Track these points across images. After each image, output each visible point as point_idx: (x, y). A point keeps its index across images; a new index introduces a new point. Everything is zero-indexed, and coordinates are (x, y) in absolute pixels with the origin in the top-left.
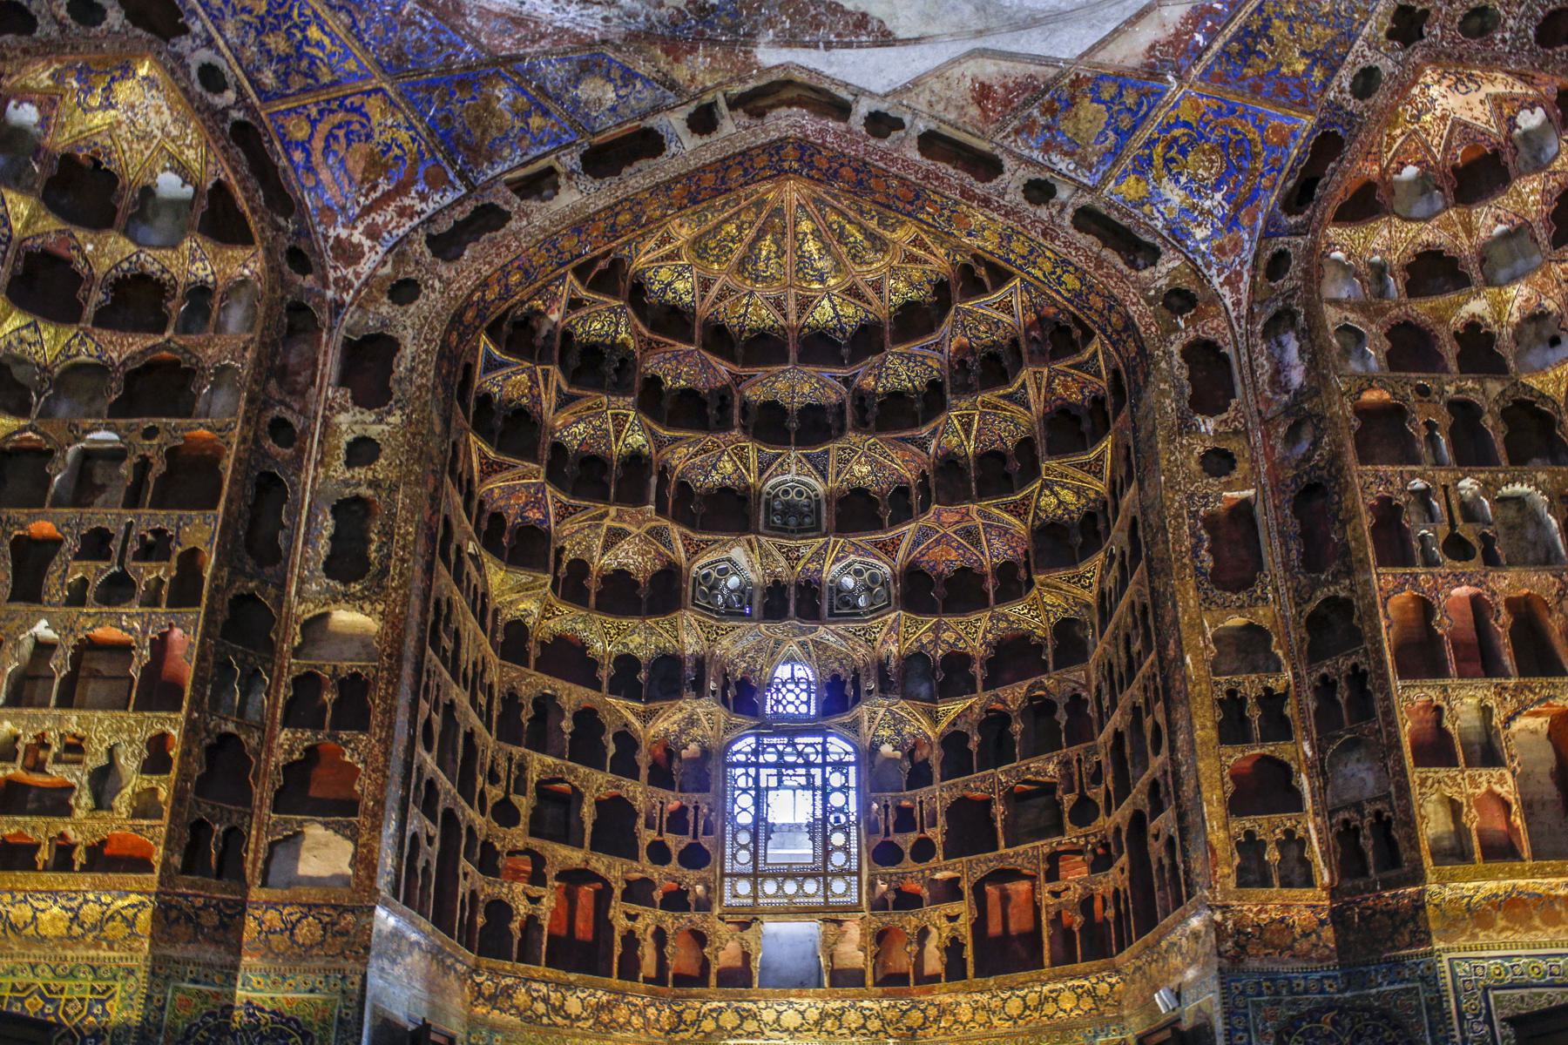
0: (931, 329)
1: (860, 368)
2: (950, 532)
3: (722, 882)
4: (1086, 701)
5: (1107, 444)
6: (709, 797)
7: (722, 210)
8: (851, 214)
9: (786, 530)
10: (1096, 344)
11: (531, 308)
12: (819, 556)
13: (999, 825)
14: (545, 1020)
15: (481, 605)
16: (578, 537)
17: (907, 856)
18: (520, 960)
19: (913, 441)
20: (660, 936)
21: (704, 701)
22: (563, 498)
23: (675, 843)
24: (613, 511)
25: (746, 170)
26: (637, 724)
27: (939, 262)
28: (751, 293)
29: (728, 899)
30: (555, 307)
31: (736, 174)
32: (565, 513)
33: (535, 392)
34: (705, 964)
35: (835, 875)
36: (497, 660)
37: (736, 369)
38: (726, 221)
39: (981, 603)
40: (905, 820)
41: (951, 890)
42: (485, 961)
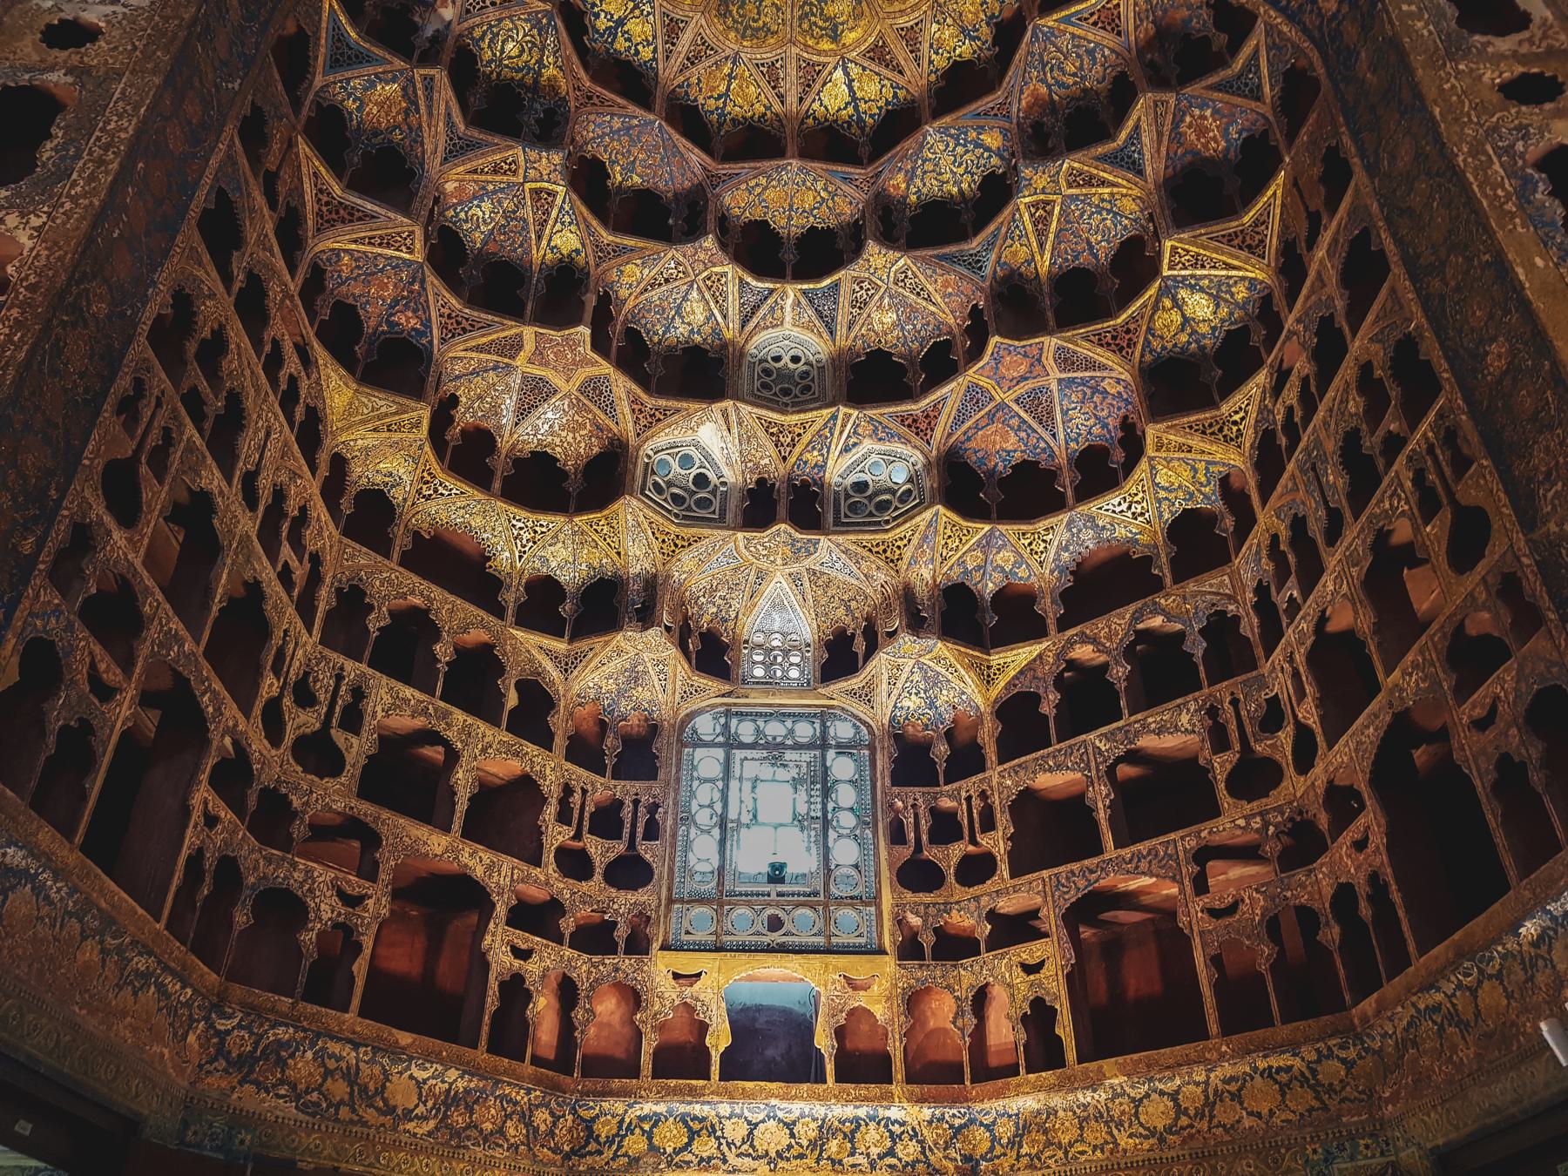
0: (990, 88)
2: (1009, 398)
3: (668, 909)
5: (1276, 188)
6: (657, 787)
12: (821, 441)
13: (1102, 816)
14: (344, 1112)
15: (310, 432)
17: (951, 879)
18: (310, 997)
20: (568, 992)
21: (654, 635)
23: (600, 850)
24: (529, 333)
26: (554, 673)
32: (456, 328)
33: (413, 120)
35: (841, 901)
36: (336, 533)
39: (1056, 504)
42: (238, 990)
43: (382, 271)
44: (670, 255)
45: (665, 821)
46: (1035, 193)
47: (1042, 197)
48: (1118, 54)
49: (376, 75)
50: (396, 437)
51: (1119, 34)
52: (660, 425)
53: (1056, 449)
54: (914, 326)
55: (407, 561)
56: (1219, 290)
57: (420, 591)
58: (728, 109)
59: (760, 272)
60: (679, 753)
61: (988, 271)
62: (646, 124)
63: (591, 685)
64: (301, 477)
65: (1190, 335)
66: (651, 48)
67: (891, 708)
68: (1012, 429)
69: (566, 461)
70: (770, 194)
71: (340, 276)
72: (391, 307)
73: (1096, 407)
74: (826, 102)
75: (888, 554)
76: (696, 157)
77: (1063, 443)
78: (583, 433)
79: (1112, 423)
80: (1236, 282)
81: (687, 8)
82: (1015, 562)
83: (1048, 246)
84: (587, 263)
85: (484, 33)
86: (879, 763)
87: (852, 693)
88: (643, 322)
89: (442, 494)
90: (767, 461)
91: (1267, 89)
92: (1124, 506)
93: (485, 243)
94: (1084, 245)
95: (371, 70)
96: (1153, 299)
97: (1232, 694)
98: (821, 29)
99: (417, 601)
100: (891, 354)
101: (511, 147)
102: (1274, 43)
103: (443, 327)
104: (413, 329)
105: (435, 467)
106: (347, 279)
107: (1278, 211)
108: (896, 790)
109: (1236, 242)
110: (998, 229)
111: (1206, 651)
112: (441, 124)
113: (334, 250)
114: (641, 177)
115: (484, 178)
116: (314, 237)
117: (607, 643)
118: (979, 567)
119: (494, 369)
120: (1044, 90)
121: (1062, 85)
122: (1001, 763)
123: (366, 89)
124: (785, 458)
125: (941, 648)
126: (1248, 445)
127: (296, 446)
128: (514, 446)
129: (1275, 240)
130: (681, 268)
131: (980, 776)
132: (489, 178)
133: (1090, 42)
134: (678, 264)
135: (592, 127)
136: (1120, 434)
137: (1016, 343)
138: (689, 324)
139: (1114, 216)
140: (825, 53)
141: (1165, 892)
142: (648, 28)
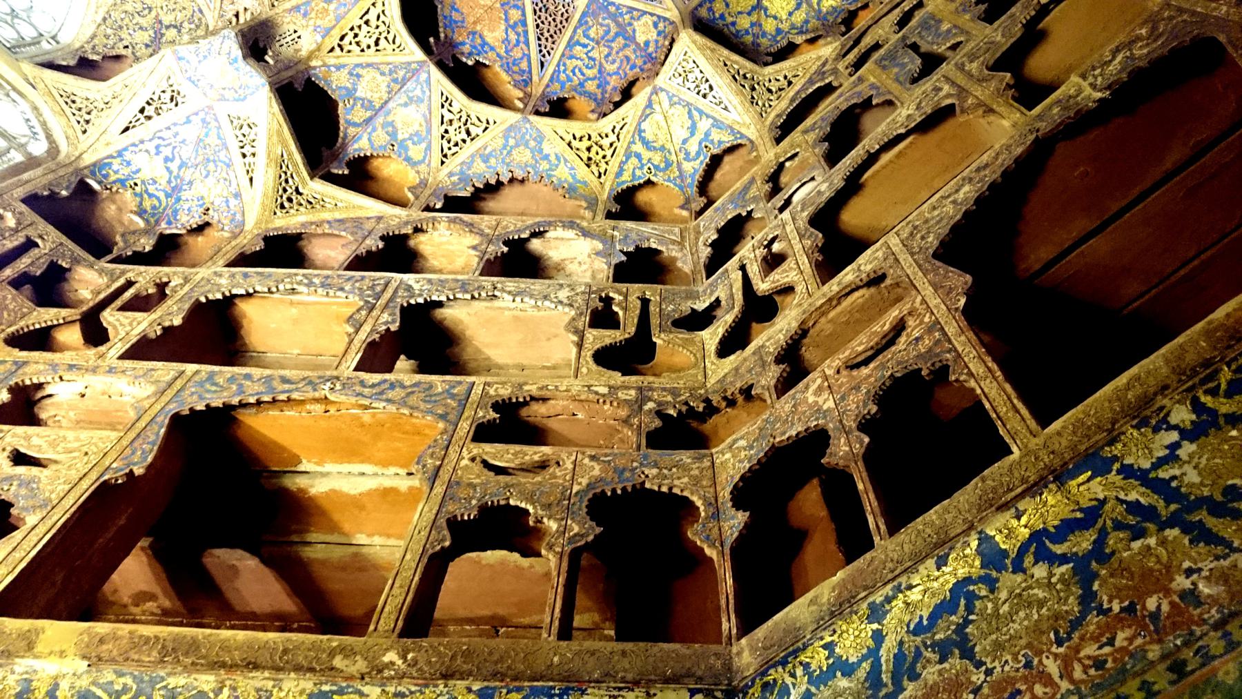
53: (535, 78)
65: (753, 25)
67: (112, 150)
68: (507, 20)
73: (607, 56)
82: (417, 134)
126: (773, 115)
141: (361, 539)
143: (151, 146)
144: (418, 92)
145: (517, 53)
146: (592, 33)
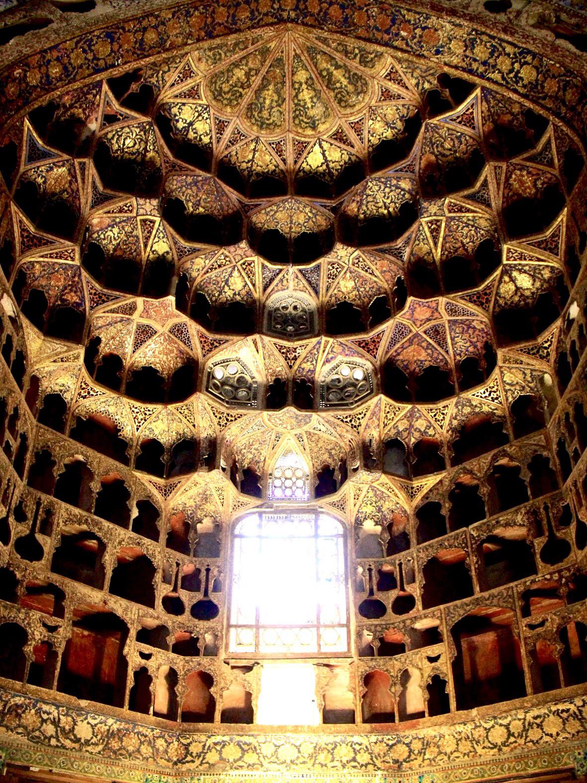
1: (346, 197)
4: (547, 460)
5: (563, 218)
7: (233, 51)
8: (338, 56)
9: (285, 334)
10: (549, 132)
11: (73, 115)
12: (312, 356)
16: (112, 330)
19: (389, 251)
21: (216, 474)
22: (97, 286)
23: (188, 598)
24: (140, 301)
25: (252, 12)
26: (158, 496)
27: (410, 97)
28: (257, 140)
29: (233, 648)
30: (93, 117)
31: (244, 15)
32: (99, 300)
33: (74, 186)
34: (211, 703)
36: (35, 422)
37: (246, 200)
38: (236, 65)
40: (387, 581)
41: (431, 636)
43: (57, 271)
44: (221, 252)
45: (225, 580)
46: (431, 216)
47: (435, 218)
48: (474, 139)
49: (54, 164)
50: (66, 364)
51: (474, 128)
52: (217, 349)
53: (448, 360)
54: (365, 288)
55: (74, 435)
56: (535, 272)
57: (81, 453)
58: (254, 168)
59: (273, 259)
60: (232, 541)
61: (405, 258)
62: (206, 179)
63: (180, 502)
64: (14, 392)
65: (520, 297)
66: (209, 136)
67: (356, 512)
68: (423, 348)
69: (163, 372)
70: (279, 215)
71: (34, 276)
72: (63, 291)
73: (470, 336)
74: (310, 163)
75: (353, 423)
76: (234, 195)
77: (452, 356)
78: (172, 355)
79: (479, 345)
80: (544, 268)
81: (229, 114)
82: (427, 426)
83: (440, 245)
84: (173, 259)
85: (114, 135)
86: (349, 545)
87: (333, 504)
88: (206, 289)
89: (92, 395)
90: (280, 369)
91: (556, 161)
92: (487, 394)
93: (115, 250)
94: (460, 244)
95: (51, 161)
96: (498, 277)
97: (545, 503)
98: (306, 123)
99: (80, 458)
100: (351, 305)
101: (129, 198)
102: (559, 136)
103: (92, 300)
104: (75, 302)
105: (88, 380)
106: (38, 277)
107: (564, 230)
108: (359, 560)
109: (542, 246)
110: (411, 235)
111: (531, 478)
112: (90, 187)
113: (30, 262)
114: (203, 208)
115: (114, 215)
116: (20, 256)
117: (188, 479)
118: (407, 429)
119: (121, 321)
120: (433, 158)
121: (444, 155)
122: (418, 544)
123: (47, 171)
124: (291, 367)
125: (384, 478)
127: (11, 375)
128: (132, 364)
129: (563, 245)
130: (228, 259)
131: (407, 551)
132: (117, 215)
133: (458, 132)
134: (227, 256)
135: (175, 182)
136: (484, 352)
137: (423, 300)
138: (233, 290)
139: (476, 228)
140: (309, 136)
142: (207, 127)
143: (364, 504)
144: (418, 415)
145: (435, 355)
146: (457, 331)
